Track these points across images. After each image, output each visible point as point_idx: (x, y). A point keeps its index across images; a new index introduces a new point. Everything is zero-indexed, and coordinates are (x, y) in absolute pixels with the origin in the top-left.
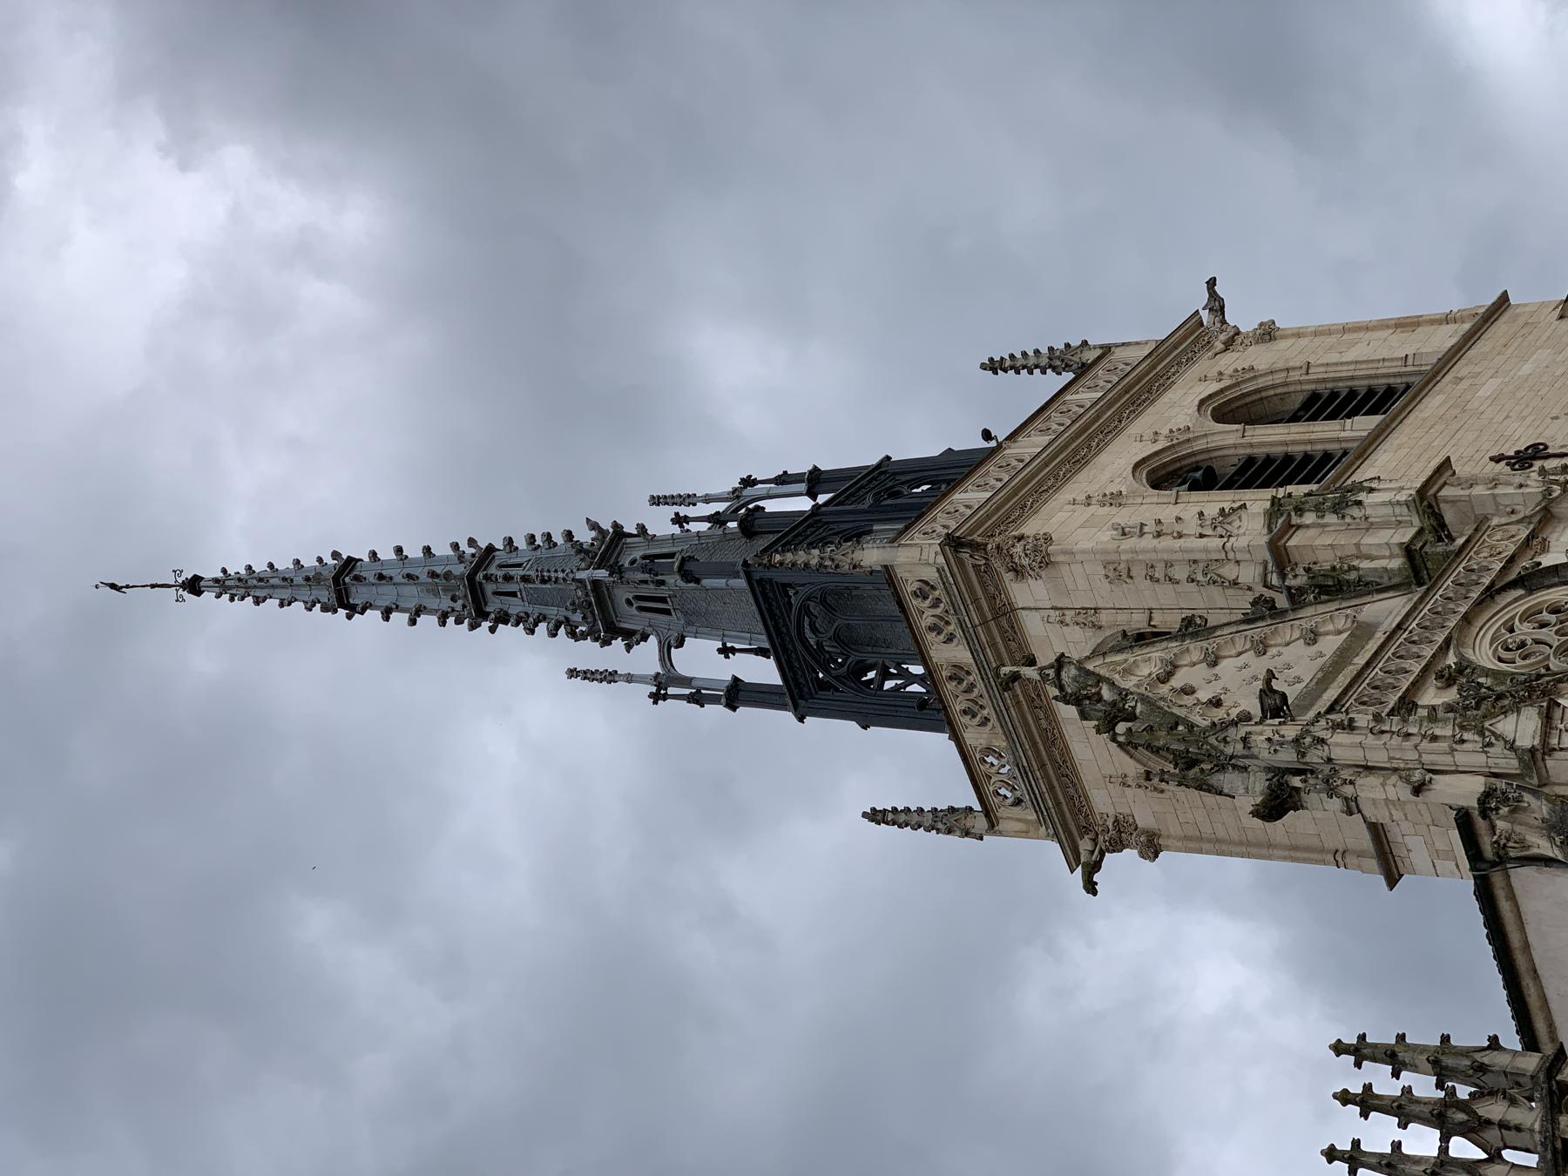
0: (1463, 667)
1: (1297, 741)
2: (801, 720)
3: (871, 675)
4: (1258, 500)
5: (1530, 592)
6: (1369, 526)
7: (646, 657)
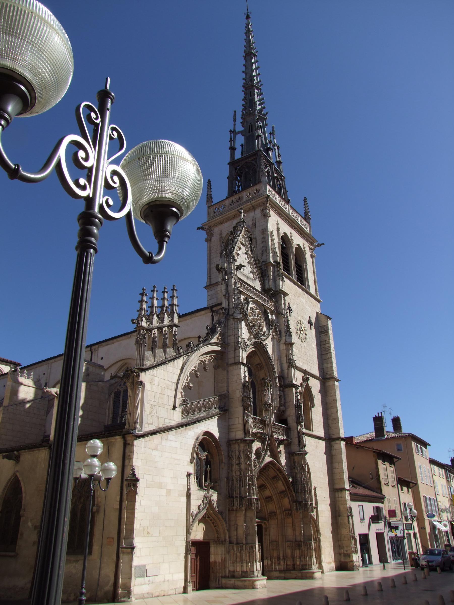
0: (248, 303)
2: (228, 164)
3: (239, 178)
7: (240, 128)
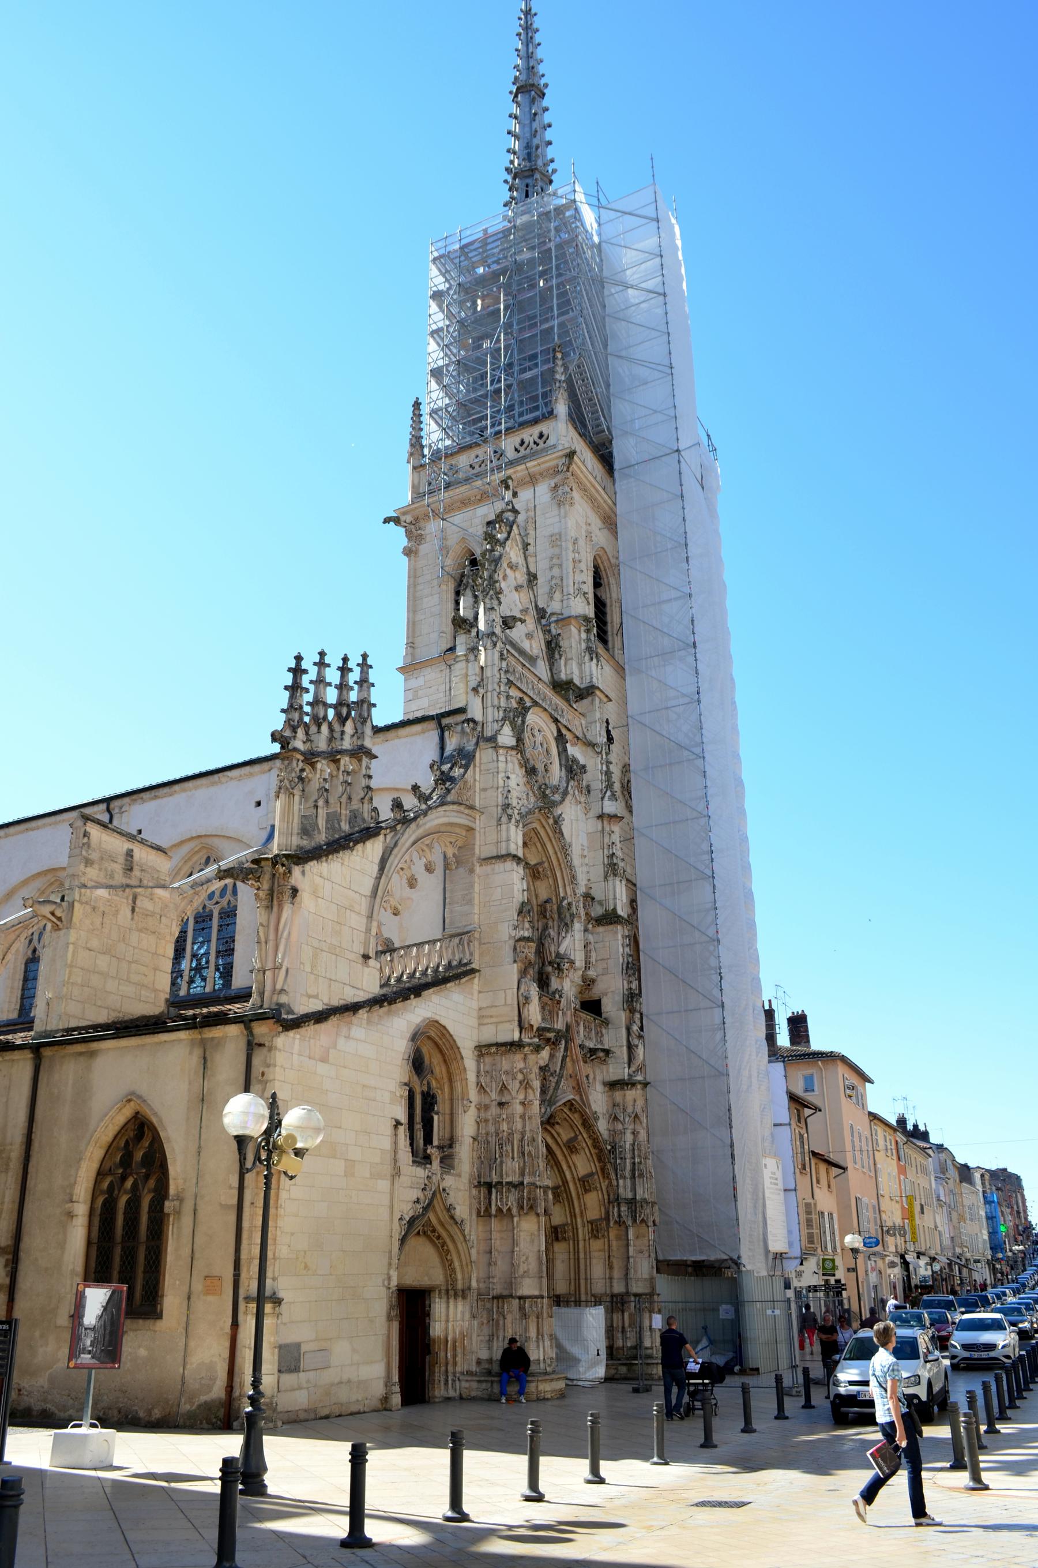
0: (526, 710)
1: (493, 633)
4: (590, 611)
5: (556, 739)
6: (580, 665)
